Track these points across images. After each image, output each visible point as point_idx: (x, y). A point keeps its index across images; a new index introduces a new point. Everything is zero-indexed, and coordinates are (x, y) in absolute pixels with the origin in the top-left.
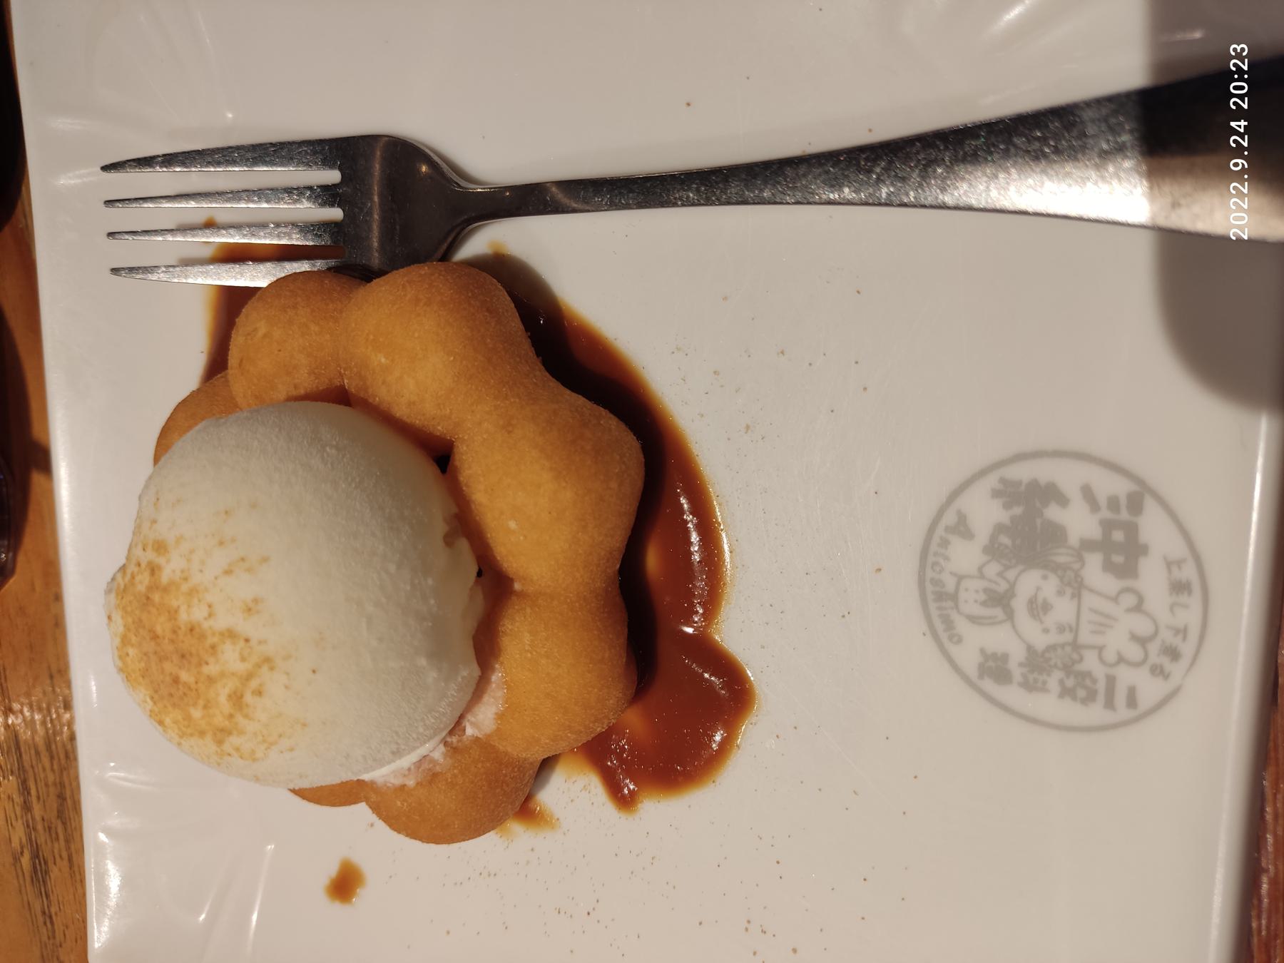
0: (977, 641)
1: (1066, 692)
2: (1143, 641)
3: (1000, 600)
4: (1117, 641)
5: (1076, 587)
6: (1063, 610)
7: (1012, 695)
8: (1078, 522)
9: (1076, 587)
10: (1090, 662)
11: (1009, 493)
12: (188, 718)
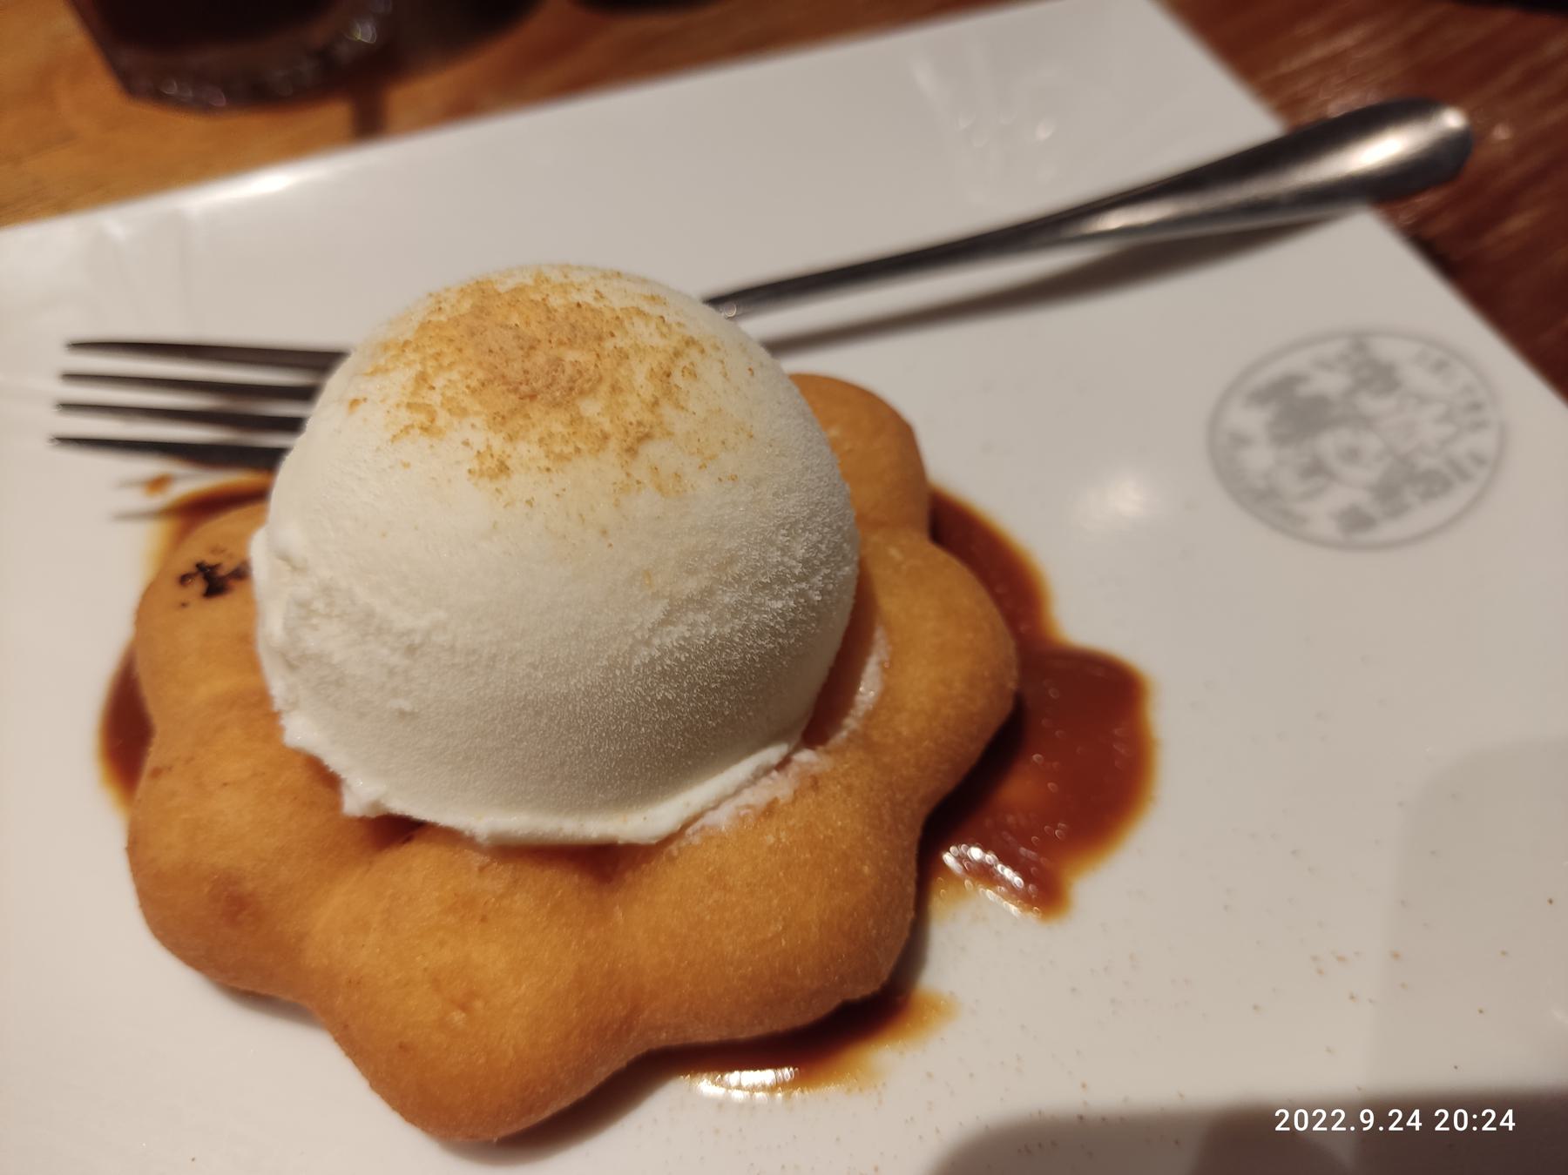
0: (1322, 512)
1: (1428, 496)
2: (1447, 418)
3: (1316, 470)
4: (1430, 430)
5: (1366, 422)
6: (1371, 443)
7: (1389, 530)
8: (1331, 383)
9: (1366, 422)
10: (1426, 462)
11: (1261, 397)
12: (576, 420)
